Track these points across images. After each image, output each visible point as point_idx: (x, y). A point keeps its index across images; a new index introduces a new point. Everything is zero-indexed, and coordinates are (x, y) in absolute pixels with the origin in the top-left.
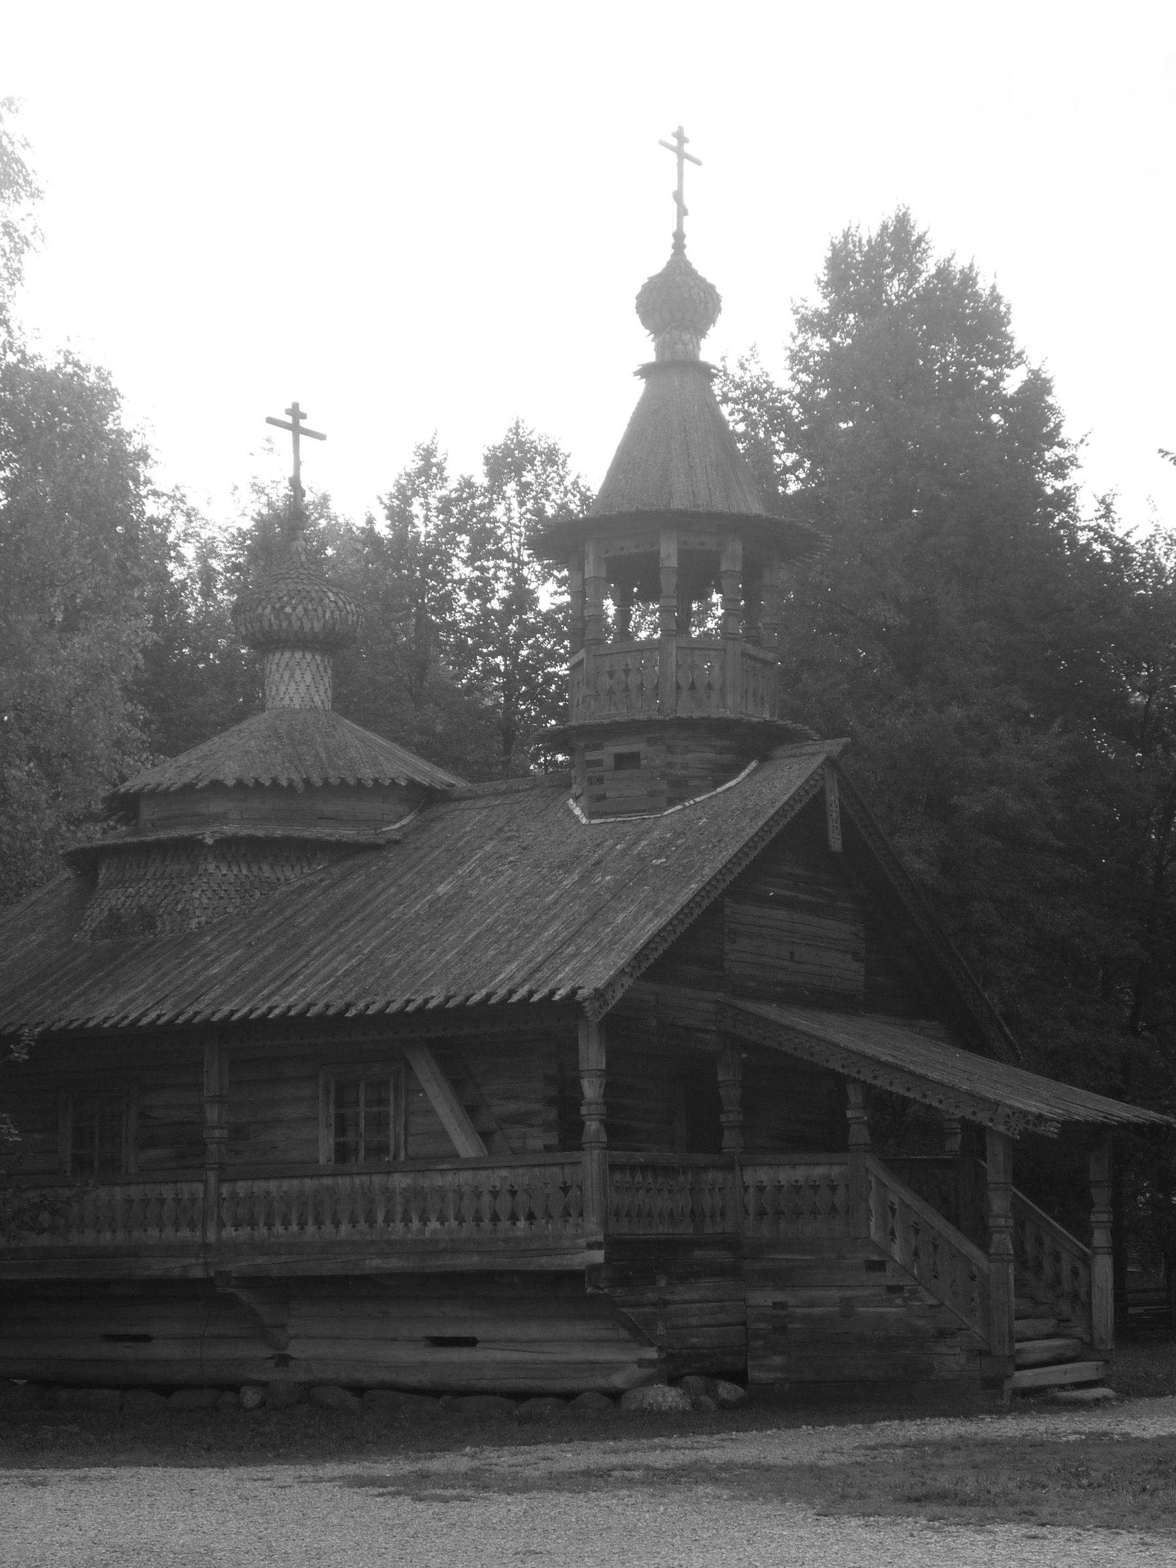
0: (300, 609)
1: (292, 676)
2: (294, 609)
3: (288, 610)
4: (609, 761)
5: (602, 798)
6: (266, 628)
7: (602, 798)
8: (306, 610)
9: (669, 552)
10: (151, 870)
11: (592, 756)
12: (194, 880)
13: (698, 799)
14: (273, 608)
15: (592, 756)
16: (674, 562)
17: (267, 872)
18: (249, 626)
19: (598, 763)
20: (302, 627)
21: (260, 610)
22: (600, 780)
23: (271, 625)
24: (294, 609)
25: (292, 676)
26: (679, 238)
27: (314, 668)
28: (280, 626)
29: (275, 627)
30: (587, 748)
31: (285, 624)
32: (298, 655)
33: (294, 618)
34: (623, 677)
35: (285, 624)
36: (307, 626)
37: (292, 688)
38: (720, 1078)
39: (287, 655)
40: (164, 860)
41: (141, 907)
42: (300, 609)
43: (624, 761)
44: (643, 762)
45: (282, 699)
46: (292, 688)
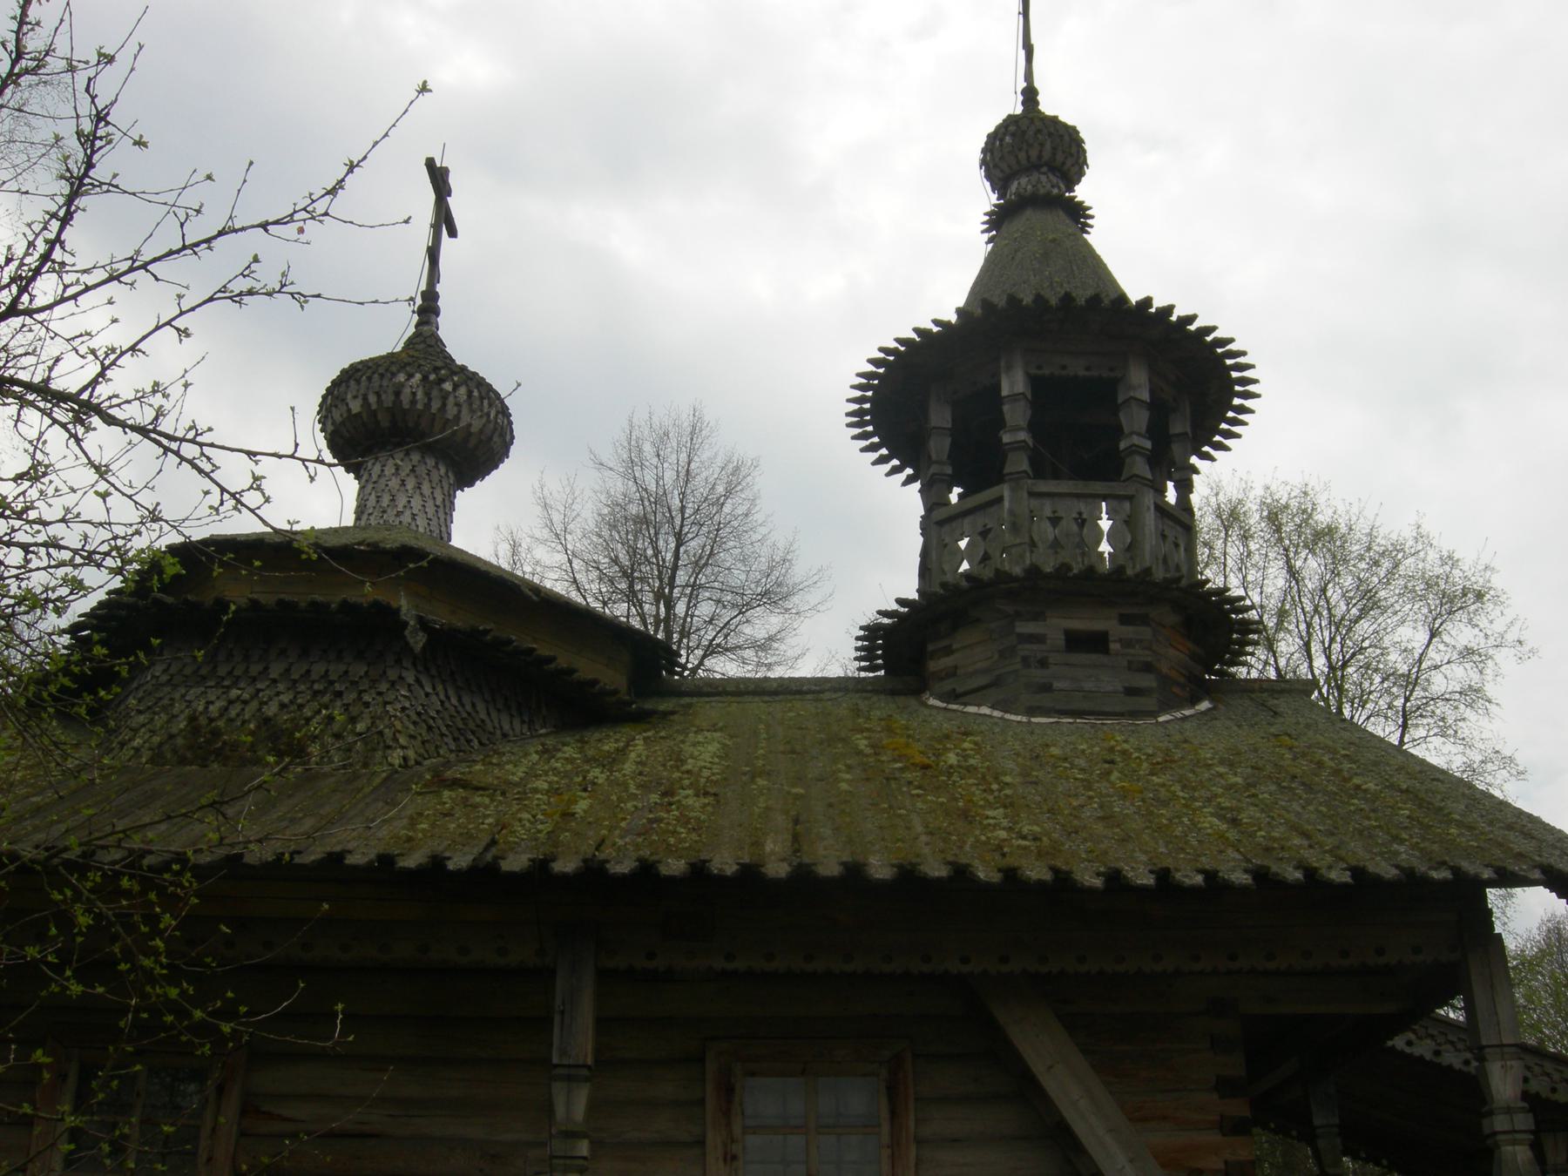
0: (462, 391)
1: (419, 487)
2: (456, 387)
3: (448, 386)
5: (1046, 688)
6: (406, 405)
8: (470, 394)
9: (1139, 382)
10: (276, 670)
12: (383, 687)
13: (1187, 712)
14: (425, 378)
17: (481, 707)
18: (372, 399)
21: (401, 377)
22: (1043, 663)
23: (413, 402)
24: (456, 387)
25: (419, 487)
26: (1030, 95)
28: (428, 406)
29: (420, 406)
31: (436, 405)
32: (431, 462)
33: (451, 400)
34: (1075, 528)
35: (436, 405)
37: (416, 503)
38: (1317, 1121)
39: (416, 457)
41: (267, 720)
42: (462, 391)
43: (1078, 642)
44: (1115, 646)
45: (399, 514)
46: (416, 503)
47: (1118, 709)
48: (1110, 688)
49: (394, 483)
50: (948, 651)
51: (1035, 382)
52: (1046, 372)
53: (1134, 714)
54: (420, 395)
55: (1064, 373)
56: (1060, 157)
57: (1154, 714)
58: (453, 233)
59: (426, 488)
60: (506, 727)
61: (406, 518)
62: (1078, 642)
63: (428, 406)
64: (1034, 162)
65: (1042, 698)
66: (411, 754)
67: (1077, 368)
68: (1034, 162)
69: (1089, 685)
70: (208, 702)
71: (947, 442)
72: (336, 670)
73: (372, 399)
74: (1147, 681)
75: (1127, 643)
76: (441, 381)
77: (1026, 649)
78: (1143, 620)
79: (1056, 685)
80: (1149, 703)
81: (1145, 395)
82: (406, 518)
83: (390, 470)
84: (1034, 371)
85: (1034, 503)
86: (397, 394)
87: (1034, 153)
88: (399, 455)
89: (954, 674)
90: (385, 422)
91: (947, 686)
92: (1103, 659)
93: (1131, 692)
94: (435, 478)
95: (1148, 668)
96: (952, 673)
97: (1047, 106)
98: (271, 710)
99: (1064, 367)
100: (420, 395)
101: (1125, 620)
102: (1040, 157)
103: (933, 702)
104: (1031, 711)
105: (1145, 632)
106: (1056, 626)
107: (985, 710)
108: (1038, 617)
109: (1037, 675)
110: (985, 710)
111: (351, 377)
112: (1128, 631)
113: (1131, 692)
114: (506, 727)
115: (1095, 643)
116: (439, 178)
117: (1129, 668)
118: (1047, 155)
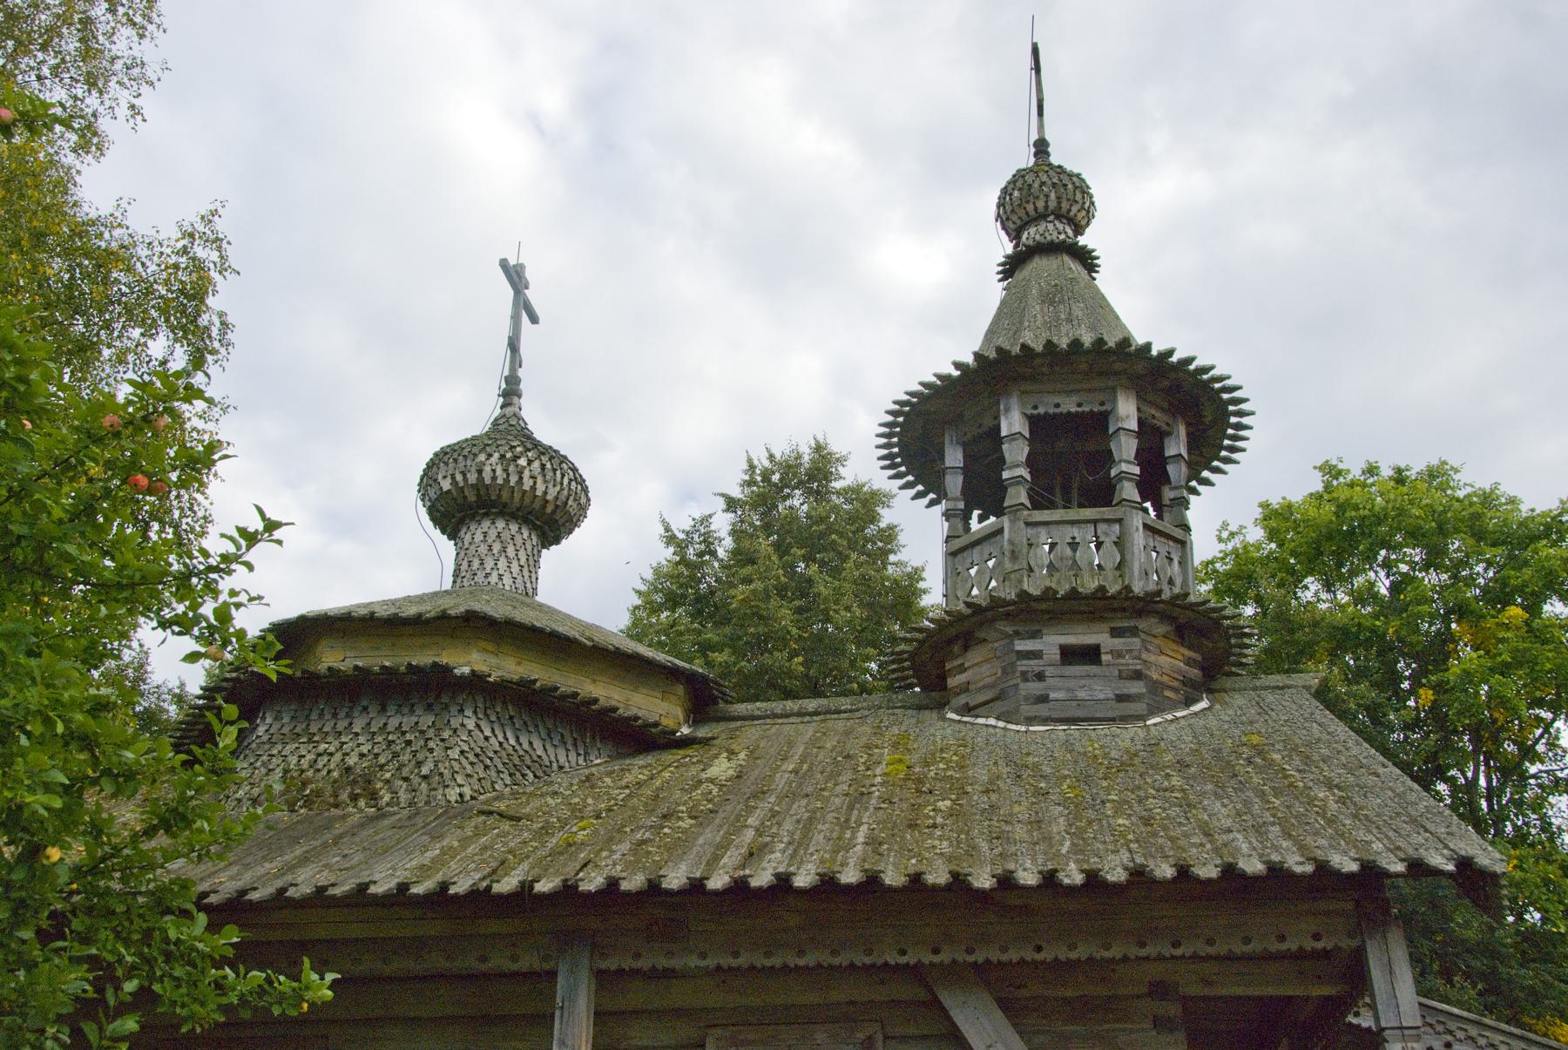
0: (536, 464)
2: (530, 462)
3: (522, 462)
4: (1053, 654)
5: (1043, 699)
6: (488, 481)
7: (1043, 699)
8: (543, 466)
9: (1127, 411)
11: (1020, 645)
12: (446, 735)
13: (1179, 714)
14: (503, 457)
15: (1020, 645)
16: (1133, 425)
17: (537, 744)
18: (459, 478)
19: (1036, 655)
20: (534, 488)
21: (482, 457)
22: (1040, 677)
23: (494, 478)
24: (530, 462)
26: (1041, 147)
27: (529, 548)
28: (507, 480)
29: (500, 481)
30: (1017, 633)
31: (513, 479)
32: (514, 527)
33: (526, 474)
34: (1068, 552)
35: (513, 479)
36: (540, 488)
37: (502, 563)
40: (383, 709)
41: (348, 769)
42: (536, 464)
43: (1071, 655)
44: (1104, 658)
45: (487, 576)
46: (502, 563)
47: (1110, 715)
48: (1102, 696)
49: (483, 549)
50: (962, 669)
51: (1035, 422)
52: (1041, 410)
53: (1125, 719)
54: (499, 472)
55: (1057, 411)
56: (1065, 205)
57: (1143, 718)
58: (534, 319)
59: (511, 551)
60: (562, 760)
61: (494, 579)
62: (1071, 655)
63: (507, 480)
64: (1045, 214)
65: (1042, 709)
66: (467, 791)
67: (1069, 405)
68: (1045, 214)
69: (1082, 694)
70: (299, 755)
71: (960, 478)
72: (408, 721)
73: (459, 478)
74: (1137, 688)
75: (1118, 654)
76: (516, 458)
77: (1023, 665)
78: (1134, 632)
79: (1053, 695)
80: (1138, 708)
81: (1134, 425)
82: (494, 579)
83: (479, 537)
84: (1030, 412)
85: (1030, 531)
86: (480, 472)
87: (1040, 204)
88: (486, 524)
89: (967, 690)
90: (472, 498)
91: (962, 700)
92: (1092, 669)
93: (1121, 698)
94: (519, 540)
95: (1137, 675)
96: (965, 689)
97: (1055, 159)
98: (352, 760)
99: (1057, 405)
100: (499, 472)
101: (1116, 633)
102: (1046, 207)
103: (951, 715)
104: (1030, 721)
105: (1135, 642)
106: (1051, 643)
107: (992, 721)
108: (1035, 635)
109: (1034, 687)
110: (992, 721)
111: (443, 458)
112: (1118, 643)
113: (1121, 698)
114: (562, 760)
115: (1090, 655)
116: (515, 276)
117: (1120, 677)
118: (1052, 204)
